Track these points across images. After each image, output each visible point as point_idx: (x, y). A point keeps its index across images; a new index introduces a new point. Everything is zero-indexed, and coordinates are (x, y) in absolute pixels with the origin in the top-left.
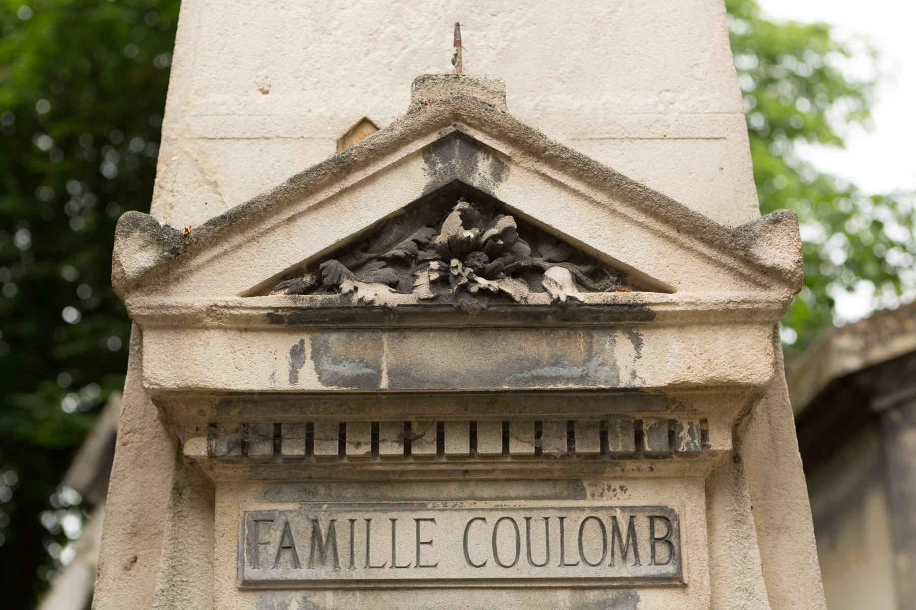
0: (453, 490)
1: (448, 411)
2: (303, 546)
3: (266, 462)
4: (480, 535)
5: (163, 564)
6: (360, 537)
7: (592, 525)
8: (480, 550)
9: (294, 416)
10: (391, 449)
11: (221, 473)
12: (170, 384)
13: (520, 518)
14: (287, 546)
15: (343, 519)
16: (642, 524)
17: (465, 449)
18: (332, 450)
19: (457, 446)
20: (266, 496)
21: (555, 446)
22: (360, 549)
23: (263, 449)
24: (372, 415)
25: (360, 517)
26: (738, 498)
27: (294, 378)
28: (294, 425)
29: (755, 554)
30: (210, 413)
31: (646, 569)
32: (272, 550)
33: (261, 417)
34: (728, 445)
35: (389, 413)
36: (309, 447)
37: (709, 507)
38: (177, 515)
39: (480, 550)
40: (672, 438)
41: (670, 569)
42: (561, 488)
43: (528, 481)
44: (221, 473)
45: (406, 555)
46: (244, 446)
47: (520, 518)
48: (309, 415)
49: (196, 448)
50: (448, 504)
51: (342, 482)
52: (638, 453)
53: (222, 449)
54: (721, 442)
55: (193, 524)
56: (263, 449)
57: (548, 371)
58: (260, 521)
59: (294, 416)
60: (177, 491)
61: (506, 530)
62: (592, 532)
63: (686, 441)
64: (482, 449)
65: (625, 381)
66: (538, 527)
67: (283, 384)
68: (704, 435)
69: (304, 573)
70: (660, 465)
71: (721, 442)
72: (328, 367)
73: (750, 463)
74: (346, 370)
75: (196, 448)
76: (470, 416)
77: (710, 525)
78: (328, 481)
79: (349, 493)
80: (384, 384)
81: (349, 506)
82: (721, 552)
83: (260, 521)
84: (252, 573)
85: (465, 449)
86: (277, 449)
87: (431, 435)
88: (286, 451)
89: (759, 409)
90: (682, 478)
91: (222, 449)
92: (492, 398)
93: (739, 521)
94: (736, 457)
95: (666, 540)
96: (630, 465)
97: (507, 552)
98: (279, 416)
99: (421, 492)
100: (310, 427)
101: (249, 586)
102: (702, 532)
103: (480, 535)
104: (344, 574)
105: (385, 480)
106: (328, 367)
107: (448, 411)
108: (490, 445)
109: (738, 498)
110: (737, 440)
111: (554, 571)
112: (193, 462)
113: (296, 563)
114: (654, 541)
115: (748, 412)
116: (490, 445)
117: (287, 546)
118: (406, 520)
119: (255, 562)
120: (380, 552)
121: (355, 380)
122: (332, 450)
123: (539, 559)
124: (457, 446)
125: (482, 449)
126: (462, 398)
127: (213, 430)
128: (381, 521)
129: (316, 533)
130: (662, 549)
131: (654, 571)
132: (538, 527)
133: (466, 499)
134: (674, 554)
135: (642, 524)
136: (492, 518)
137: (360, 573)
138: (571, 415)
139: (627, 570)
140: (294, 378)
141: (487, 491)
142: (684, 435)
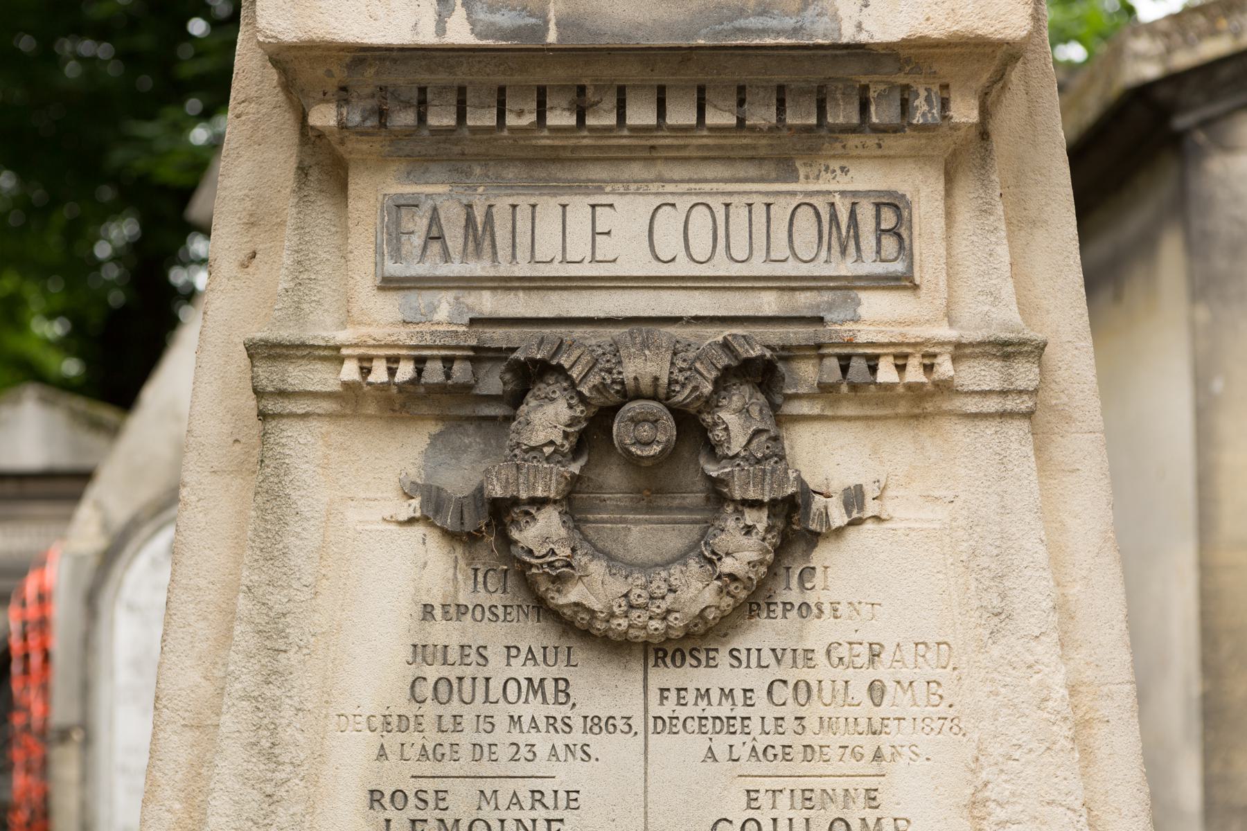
0: (636, 170)
1: (631, 72)
2: (455, 237)
3: (409, 134)
4: (669, 224)
5: (287, 259)
6: (523, 226)
7: (805, 215)
8: (669, 242)
9: (442, 78)
10: (560, 118)
11: (356, 148)
12: (290, 37)
13: (717, 204)
14: (435, 236)
15: (502, 204)
16: (866, 213)
17: (650, 119)
18: (488, 119)
19: (641, 115)
20: (409, 176)
21: (762, 116)
22: (523, 240)
23: (404, 118)
24: (538, 77)
25: (524, 202)
26: (985, 183)
27: (441, 29)
28: (442, 90)
29: (1003, 251)
30: (340, 74)
31: (870, 266)
32: (417, 241)
33: (401, 78)
34: (973, 116)
35: (557, 74)
36: (461, 116)
37: (948, 194)
38: (303, 200)
39: (669, 242)
40: (905, 107)
41: (898, 267)
42: (768, 169)
43: (728, 160)
44: (356, 148)
45: (579, 246)
46: (382, 114)
47: (717, 204)
48: (460, 77)
49: (324, 117)
50: (628, 186)
51: (502, 160)
52: (863, 126)
53: (355, 118)
54: (965, 112)
55: (322, 212)
56: (404, 118)
57: (754, 22)
58: (403, 206)
59: (442, 78)
60: (303, 171)
61: (700, 219)
62: (805, 220)
63: (922, 111)
64: (673, 119)
65: (848, 35)
66: (739, 216)
67: (427, 37)
68: (945, 104)
69: (456, 269)
70: (890, 141)
71: (965, 112)
72: (482, 16)
73: (1001, 142)
74: (505, 19)
75: (324, 117)
76: (658, 78)
77: (949, 215)
78: (485, 159)
79: (510, 173)
80: (552, 37)
81: (511, 188)
82: (962, 247)
83: (403, 206)
84: (394, 269)
85: (650, 119)
86: (422, 118)
87: (610, 101)
88: (433, 121)
89: (1015, 76)
90: (916, 156)
91: (355, 118)
92: (684, 56)
93: (985, 212)
94: (983, 133)
95: (895, 232)
96: (853, 140)
97: (701, 244)
98: (424, 78)
99: (597, 172)
100: (462, 91)
101: (389, 284)
102: (939, 224)
103: (669, 224)
104: (505, 270)
105: (554, 157)
106: (482, 16)
107: (631, 72)
108: (681, 114)
109: (985, 183)
110: (985, 112)
111: (758, 267)
112: (320, 134)
113: (446, 257)
114: (880, 232)
115: (1000, 77)
116: (681, 114)
117: (435, 236)
118: (579, 207)
119: (397, 256)
120: (548, 245)
121: (516, 33)
122: (488, 119)
123: (740, 252)
124: (641, 115)
125: (673, 119)
126: (647, 55)
127: (343, 95)
128: (549, 207)
129: (470, 221)
130: (889, 244)
131: (880, 269)
132: (739, 216)
133: (652, 181)
134: (904, 248)
135: (866, 213)
136: (684, 204)
137: (523, 269)
138: (781, 78)
139: (847, 268)
140: (441, 29)
141: (678, 171)
142: (920, 103)
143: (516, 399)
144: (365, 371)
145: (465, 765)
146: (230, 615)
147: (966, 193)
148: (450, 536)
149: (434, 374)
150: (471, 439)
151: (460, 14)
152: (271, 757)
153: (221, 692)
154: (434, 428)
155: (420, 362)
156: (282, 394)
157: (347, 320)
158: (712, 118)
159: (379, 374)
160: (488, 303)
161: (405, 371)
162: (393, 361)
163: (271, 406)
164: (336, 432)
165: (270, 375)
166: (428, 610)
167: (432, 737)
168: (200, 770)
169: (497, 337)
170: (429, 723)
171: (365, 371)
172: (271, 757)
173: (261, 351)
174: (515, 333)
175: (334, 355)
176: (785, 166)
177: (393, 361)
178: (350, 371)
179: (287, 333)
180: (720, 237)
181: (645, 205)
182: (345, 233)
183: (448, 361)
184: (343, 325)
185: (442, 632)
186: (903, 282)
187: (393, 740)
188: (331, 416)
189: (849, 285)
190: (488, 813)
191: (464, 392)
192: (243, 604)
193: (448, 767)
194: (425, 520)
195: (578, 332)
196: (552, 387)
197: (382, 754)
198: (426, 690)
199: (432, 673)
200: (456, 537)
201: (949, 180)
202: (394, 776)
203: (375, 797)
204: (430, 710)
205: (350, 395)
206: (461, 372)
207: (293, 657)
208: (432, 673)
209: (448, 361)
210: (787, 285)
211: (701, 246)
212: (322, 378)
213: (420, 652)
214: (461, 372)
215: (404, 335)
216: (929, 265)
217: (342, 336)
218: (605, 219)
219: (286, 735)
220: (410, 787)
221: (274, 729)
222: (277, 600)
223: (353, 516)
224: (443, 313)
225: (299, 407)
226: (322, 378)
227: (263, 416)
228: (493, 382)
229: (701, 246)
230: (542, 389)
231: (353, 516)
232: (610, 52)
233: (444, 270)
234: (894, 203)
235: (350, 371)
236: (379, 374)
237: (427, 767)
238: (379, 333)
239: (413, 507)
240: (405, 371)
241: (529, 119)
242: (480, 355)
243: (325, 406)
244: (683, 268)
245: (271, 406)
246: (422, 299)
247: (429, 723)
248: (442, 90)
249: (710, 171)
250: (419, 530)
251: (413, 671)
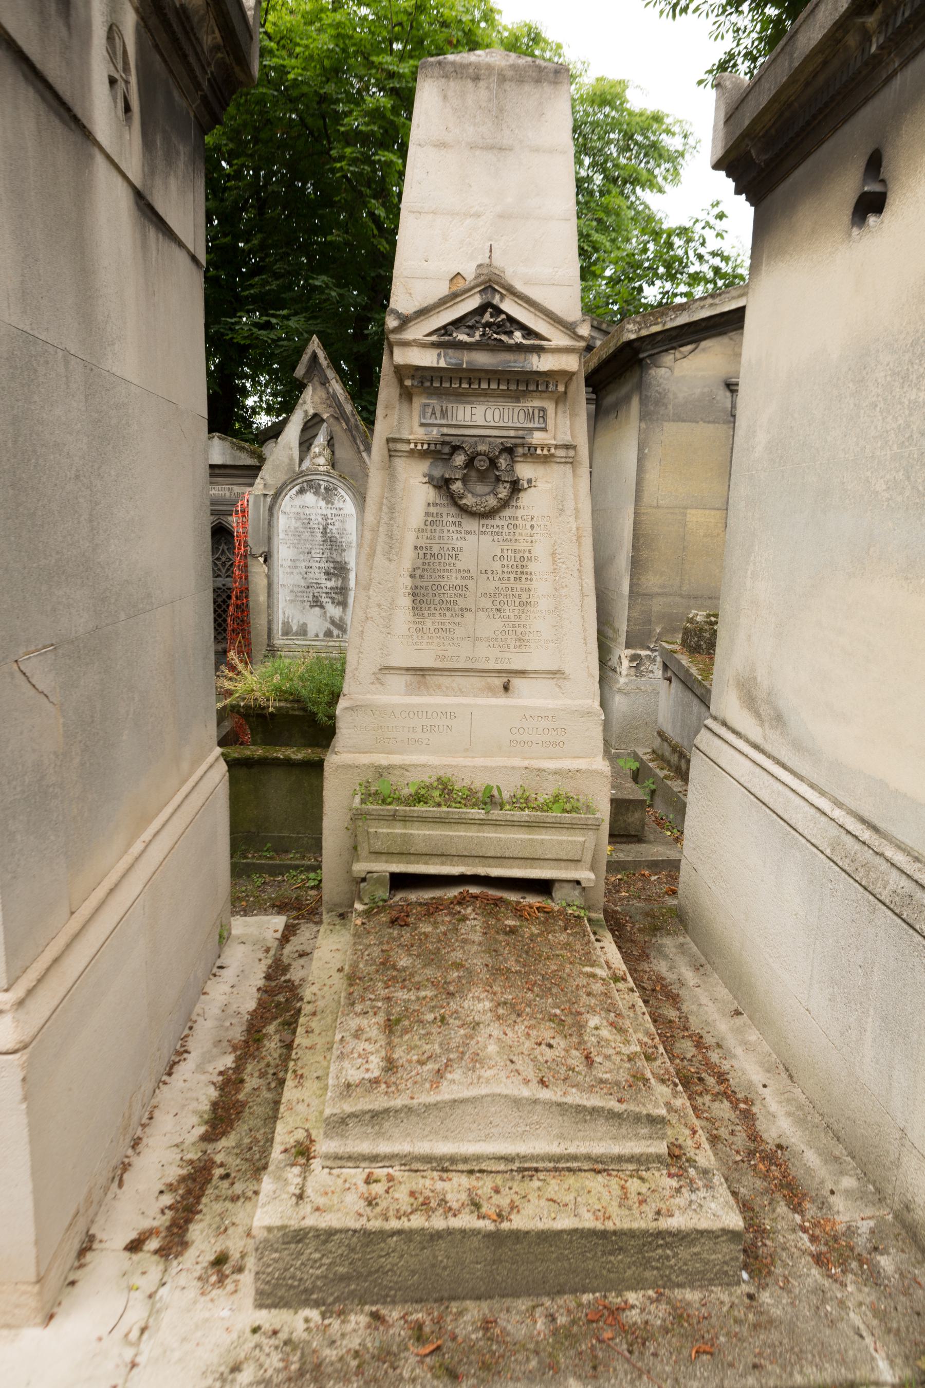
0: (482, 399)
1: (483, 375)
2: (438, 414)
3: (428, 388)
4: (490, 413)
5: (396, 417)
6: (455, 411)
7: (522, 412)
8: (489, 417)
9: (437, 374)
10: (465, 386)
11: (415, 390)
12: (401, 363)
13: (501, 408)
14: (433, 413)
15: (450, 406)
16: (536, 412)
17: (486, 387)
18: (448, 385)
19: (484, 386)
20: (427, 398)
21: (513, 387)
22: (455, 415)
23: (428, 384)
24: (460, 375)
25: (455, 406)
26: (565, 405)
27: (438, 363)
28: (437, 377)
29: (568, 422)
30: (412, 372)
31: (536, 425)
32: (429, 414)
33: (427, 374)
34: (563, 389)
35: (464, 375)
36: (441, 384)
37: (556, 407)
38: (401, 402)
39: (489, 417)
40: (547, 386)
41: (543, 426)
42: (514, 400)
43: (504, 397)
44: (415, 390)
45: (468, 418)
46: (422, 383)
47: (501, 408)
48: (442, 374)
49: (408, 383)
50: (480, 403)
51: (449, 395)
52: (537, 391)
53: (416, 383)
54: (561, 388)
55: (405, 406)
56: (428, 384)
57: (512, 364)
58: (426, 405)
59: (437, 374)
60: (401, 395)
61: (497, 412)
62: (522, 413)
63: (551, 388)
64: (492, 387)
65: (535, 369)
66: (506, 411)
67: (435, 365)
68: (557, 386)
69: (438, 422)
70: (544, 395)
71: (561, 388)
72: (448, 360)
73: (570, 394)
74: (453, 361)
75: (408, 383)
76: (489, 376)
77: (556, 413)
78: (446, 394)
79: (452, 398)
80: (464, 366)
81: (451, 402)
82: (559, 421)
83: (426, 405)
84: (423, 421)
85: (486, 387)
86: (432, 384)
87: (477, 382)
88: (434, 385)
89: (574, 378)
90: (549, 398)
91: (416, 383)
92: (495, 372)
93: (565, 412)
94: (565, 393)
95: (543, 417)
96: (534, 394)
97: (497, 418)
98: (433, 374)
99: (473, 399)
100: (441, 378)
101: (422, 425)
102: (553, 415)
103: (490, 413)
104: (450, 422)
105: (462, 395)
106: (448, 360)
107: (483, 375)
108: (494, 386)
109: (565, 405)
110: (566, 387)
111: (510, 424)
112: (406, 387)
113: (436, 419)
114: (539, 417)
115: (571, 379)
116: (494, 386)
117: (433, 413)
118: (468, 407)
119: (424, 418)
120: (460, 417)
121: (456, 364)
122: (448, 385)
123: (506, 420)
124: (484, 386)
125: (492, 387)
126: (487, 371)
127: (413, 377)
128: (461, 407)
129: (442, 410)
130: (541, 420)
131: (539, 426)
132: (506, 411)
134: (545, 421)
135: (536, 412)
136: (493, 408)
137: (454, 422)
138: (518, 378)
139: (531, 425)
140: (438, 363)
141: (492, 399)
142: (551, 385)
143: (452, 454)
144: (416, 446)
145: (437, 541)
146: (382, 504)
147: (560, 407)
148: (435, 487)
149: (432, 447)
150: (440, 463)
151: (443, 359)
152: (391, 538)
153: (379, 523)
154: (431, 460)
155: (429, 444)
156: (395, 451)
157: (411, 433)
158: (501, 387)
159: (419, 447)
160: (445, 430)
161: (426, 446)
162: (422, 444)
163: (393, 454)
164: (408, 461)
165: (392, 446)
166: (429, 504)
167: (429, 534)
168: (374, 541)
169: (447, 439)
170: (429, 531)
171: (416, 446)
172: (391, 538)
173: (389, 440)
174: (452, 438)
175: (408, 442)
176: (517, 399)
177: (422, 444)
178: (412, 446)
179: (397, 436)
180: (501, 416)
181: (484, 408)
182: (411, 411)
183: (436, 444)
184: (410, 434)
185: (432, 509)
186: (544, 429)
187: (420, 534)
188: (407, 457)
189: (531, 430)
190: (442, 552)
191: (439, 452)
192: (385, 501)
193: (433, 541)
194: (429, 483)
195: (467, 438)
196: (461, 452)
197: (418, 537)
198: (428, 523)
199: (430, 519)
200: (437, 487)
201: (557, 404)
202: (421, 543)
203: (416, 547)
204: (429, 527)
205: (412, 452)
206: (439, 447)
207: (397, 514)
208: (430, 519)
209: (436, 444)
210: (517, 429)
211: (497, 419)
212: (405, 447)
213: (427, 514)
214: (439, 447)
215: (425, 438)
216: (550, 426)
217: (411, 437)
218: (474, 411)
219: (395, 533)
220: (424, 545)
221: (392, 531)
222: (393, 500)
223: (412, 481)
224: (435, 432)
225: (399, 454)
226: (405, 447)
227: (390, 456)
228: (447, 450)
229: (497, 419)
230: (458, 452)
231: (412, 481)
232: (478, 370)
233: (435, 422)
234: (543, 410)
235: (412, 446)
236: (419, 447)
237: (428, 541)
238: (420, 437)
239: (426, 479)
240: (426, 446)
241: (457, 385)
242: (444, 443)
243: (405, 454)
244: (492, 424)
245: (393, 454)
246: (430, 429)
247: (429, 531)
248: (437, 377)
249: (499, 400)
250: (427, 485)
251: (425, 519)
